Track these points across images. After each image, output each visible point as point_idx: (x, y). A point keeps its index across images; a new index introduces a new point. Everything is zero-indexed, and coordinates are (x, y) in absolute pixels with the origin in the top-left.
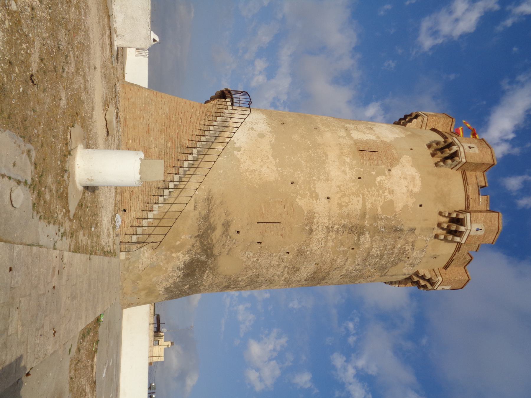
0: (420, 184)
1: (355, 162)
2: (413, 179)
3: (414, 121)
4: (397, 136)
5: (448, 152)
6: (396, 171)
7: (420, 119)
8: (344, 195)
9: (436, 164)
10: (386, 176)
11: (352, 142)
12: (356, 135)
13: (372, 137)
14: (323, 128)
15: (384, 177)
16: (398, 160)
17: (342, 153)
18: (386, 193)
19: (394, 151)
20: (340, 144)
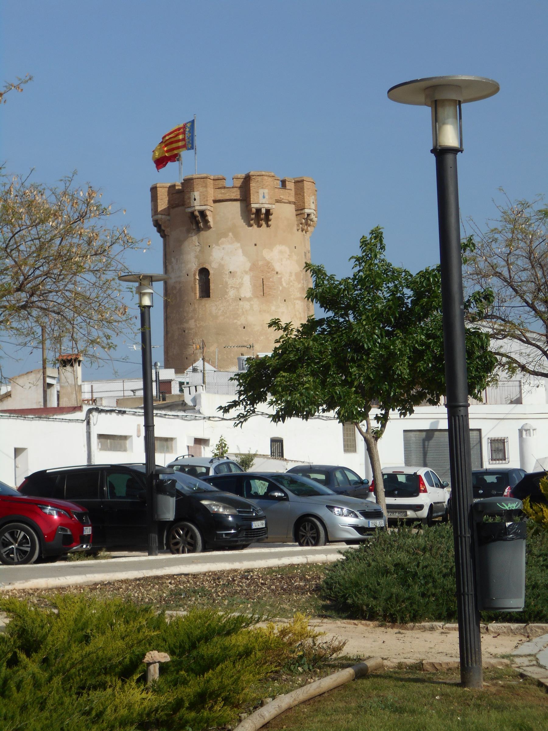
0: (284, 246)
1: (274, 303)
2: (281, 252)
3: (210, 218)
4: (240, 251)
5: (263, 216)
6: (278, 268)
7: (208, 213)
8: (295, 315)
9: (268, 226)
10: (281, 278)
11: (255, 300)
12: (247, 291)
13: (247, 279)
14: (242, 321)
15: (283, 280)
16: (268, 263)
17: (268, 312)
18: (292, 279)
19: (260, 263)
20: (260, 311)
